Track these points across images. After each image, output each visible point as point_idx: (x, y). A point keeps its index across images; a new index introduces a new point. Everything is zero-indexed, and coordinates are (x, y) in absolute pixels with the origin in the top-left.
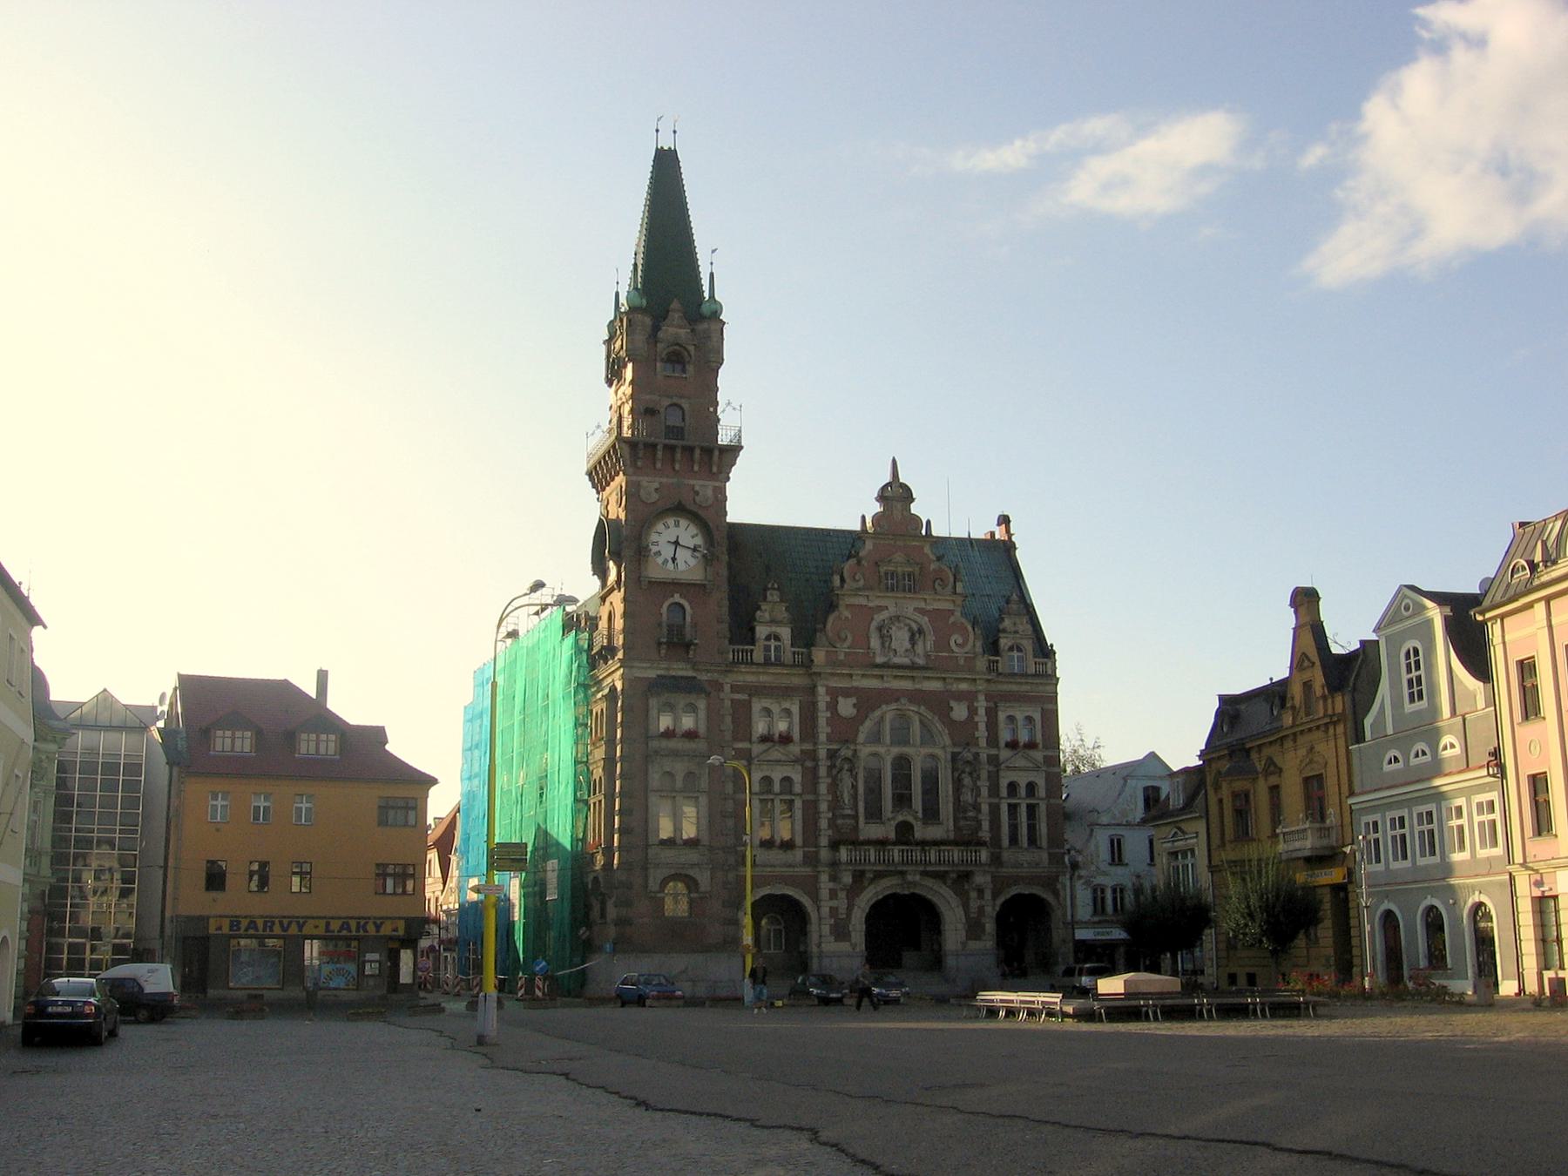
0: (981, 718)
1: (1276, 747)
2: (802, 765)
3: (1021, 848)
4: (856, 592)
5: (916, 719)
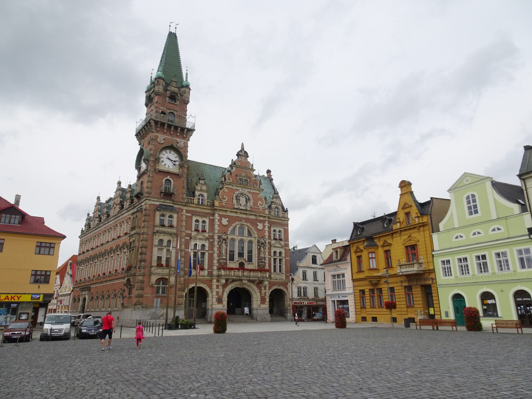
0: (267, 229)
1: (390, 237)
2: (209, 240)
3: (277, 273)
4: (229, 184)
5: (247, 227)
